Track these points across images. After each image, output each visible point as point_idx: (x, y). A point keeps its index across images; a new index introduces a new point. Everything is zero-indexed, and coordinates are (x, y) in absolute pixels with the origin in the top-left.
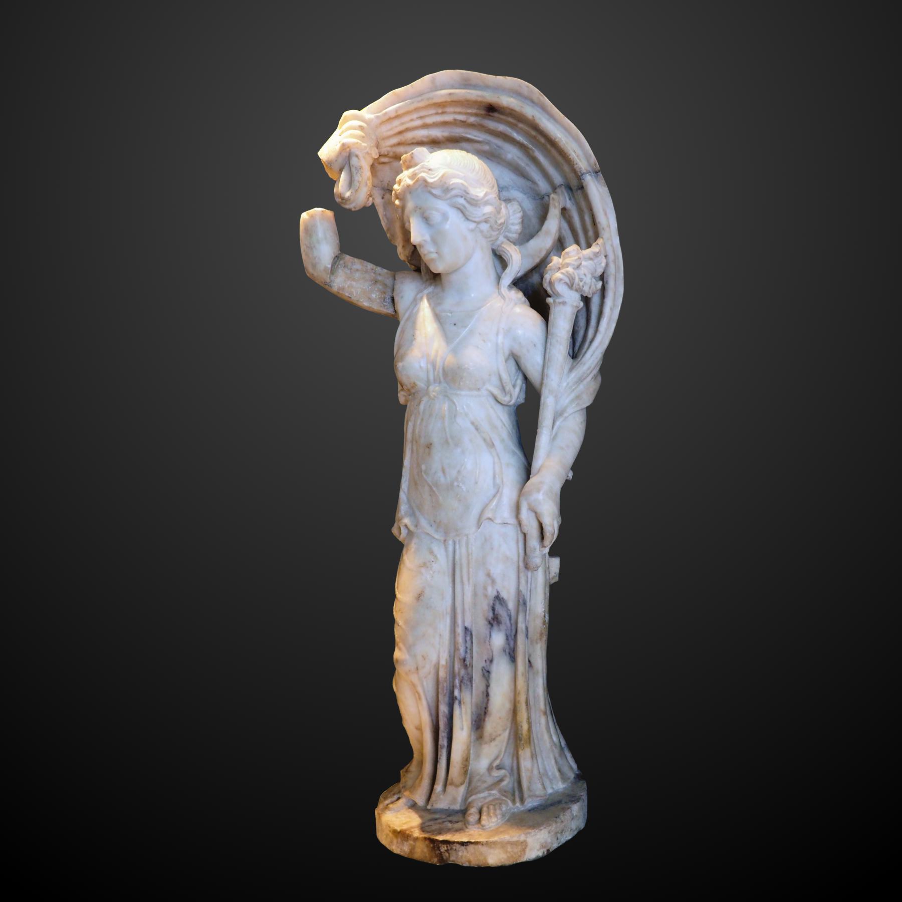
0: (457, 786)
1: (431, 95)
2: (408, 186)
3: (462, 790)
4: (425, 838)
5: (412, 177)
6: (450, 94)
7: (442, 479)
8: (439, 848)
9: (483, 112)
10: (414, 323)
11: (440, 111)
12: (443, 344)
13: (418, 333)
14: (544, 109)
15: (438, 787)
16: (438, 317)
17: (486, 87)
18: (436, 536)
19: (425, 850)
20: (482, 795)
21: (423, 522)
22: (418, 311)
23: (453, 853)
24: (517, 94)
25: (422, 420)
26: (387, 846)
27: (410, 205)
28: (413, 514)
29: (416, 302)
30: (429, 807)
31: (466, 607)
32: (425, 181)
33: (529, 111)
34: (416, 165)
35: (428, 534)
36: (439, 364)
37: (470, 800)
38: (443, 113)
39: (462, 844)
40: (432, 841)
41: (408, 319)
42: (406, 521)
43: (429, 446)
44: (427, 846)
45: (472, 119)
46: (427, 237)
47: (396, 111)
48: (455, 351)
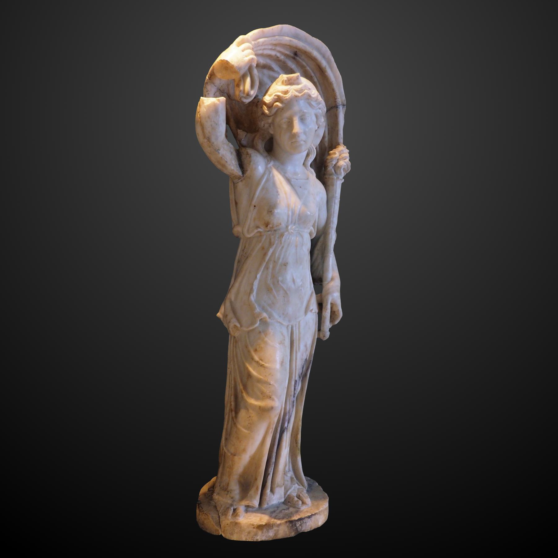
0: (281, 487)
1: (281, 38)
2: (296, 96)
3: (283, 488)
4: (286, 522)
5: (300, 91)
6: (291, 41)
7: (293, 286)
8: (295, 525)
9: (292, 55)
10: (274, 184)
11: (273, 48)
12: (298, 199)
13: (279, 190)
14: (328, 62)
15: (268, 491)
16: (289, 181)
17: (305, 41)
18: (284, 323)
19: (287, 530)
20: (293, 488)
21: (275, 315)
22: (273, 176)
23: (304, 525)
24: (319, 50)
25: (283, 247)
26: (249, 540)
27: (296, 108)
28: (266, 311)
29: (268, 170)
30: (265, 506)
31: (297, 367)
32: (310, 96)
33: (324, 63)
34: (298, 84)
35: (279, 322)
36: (297, 212)
37: (288, 493)
38: (274, 50)
39: (309, 517)
40: (291, 522)
41: (267, 180)
42: (265, 315)
43: (285, 265)
44: (288, 527)
45: (282, 57)
46: (302, 131)
47: (263, 43)
48: (305, 204)
